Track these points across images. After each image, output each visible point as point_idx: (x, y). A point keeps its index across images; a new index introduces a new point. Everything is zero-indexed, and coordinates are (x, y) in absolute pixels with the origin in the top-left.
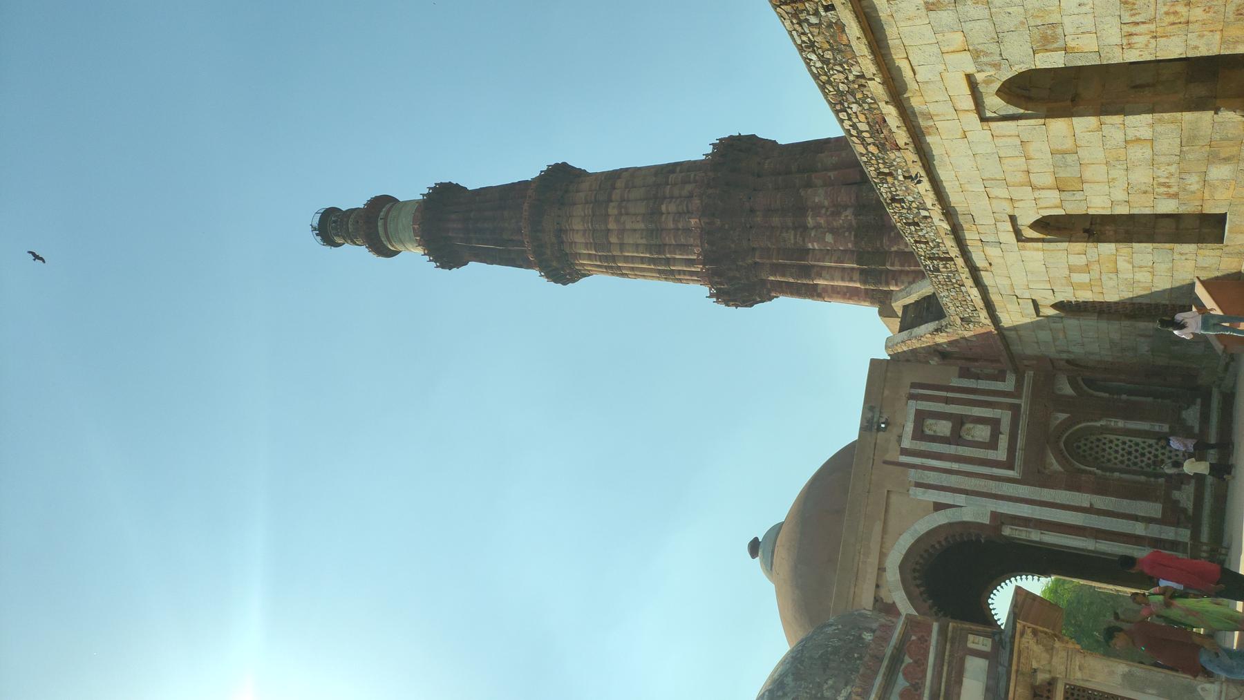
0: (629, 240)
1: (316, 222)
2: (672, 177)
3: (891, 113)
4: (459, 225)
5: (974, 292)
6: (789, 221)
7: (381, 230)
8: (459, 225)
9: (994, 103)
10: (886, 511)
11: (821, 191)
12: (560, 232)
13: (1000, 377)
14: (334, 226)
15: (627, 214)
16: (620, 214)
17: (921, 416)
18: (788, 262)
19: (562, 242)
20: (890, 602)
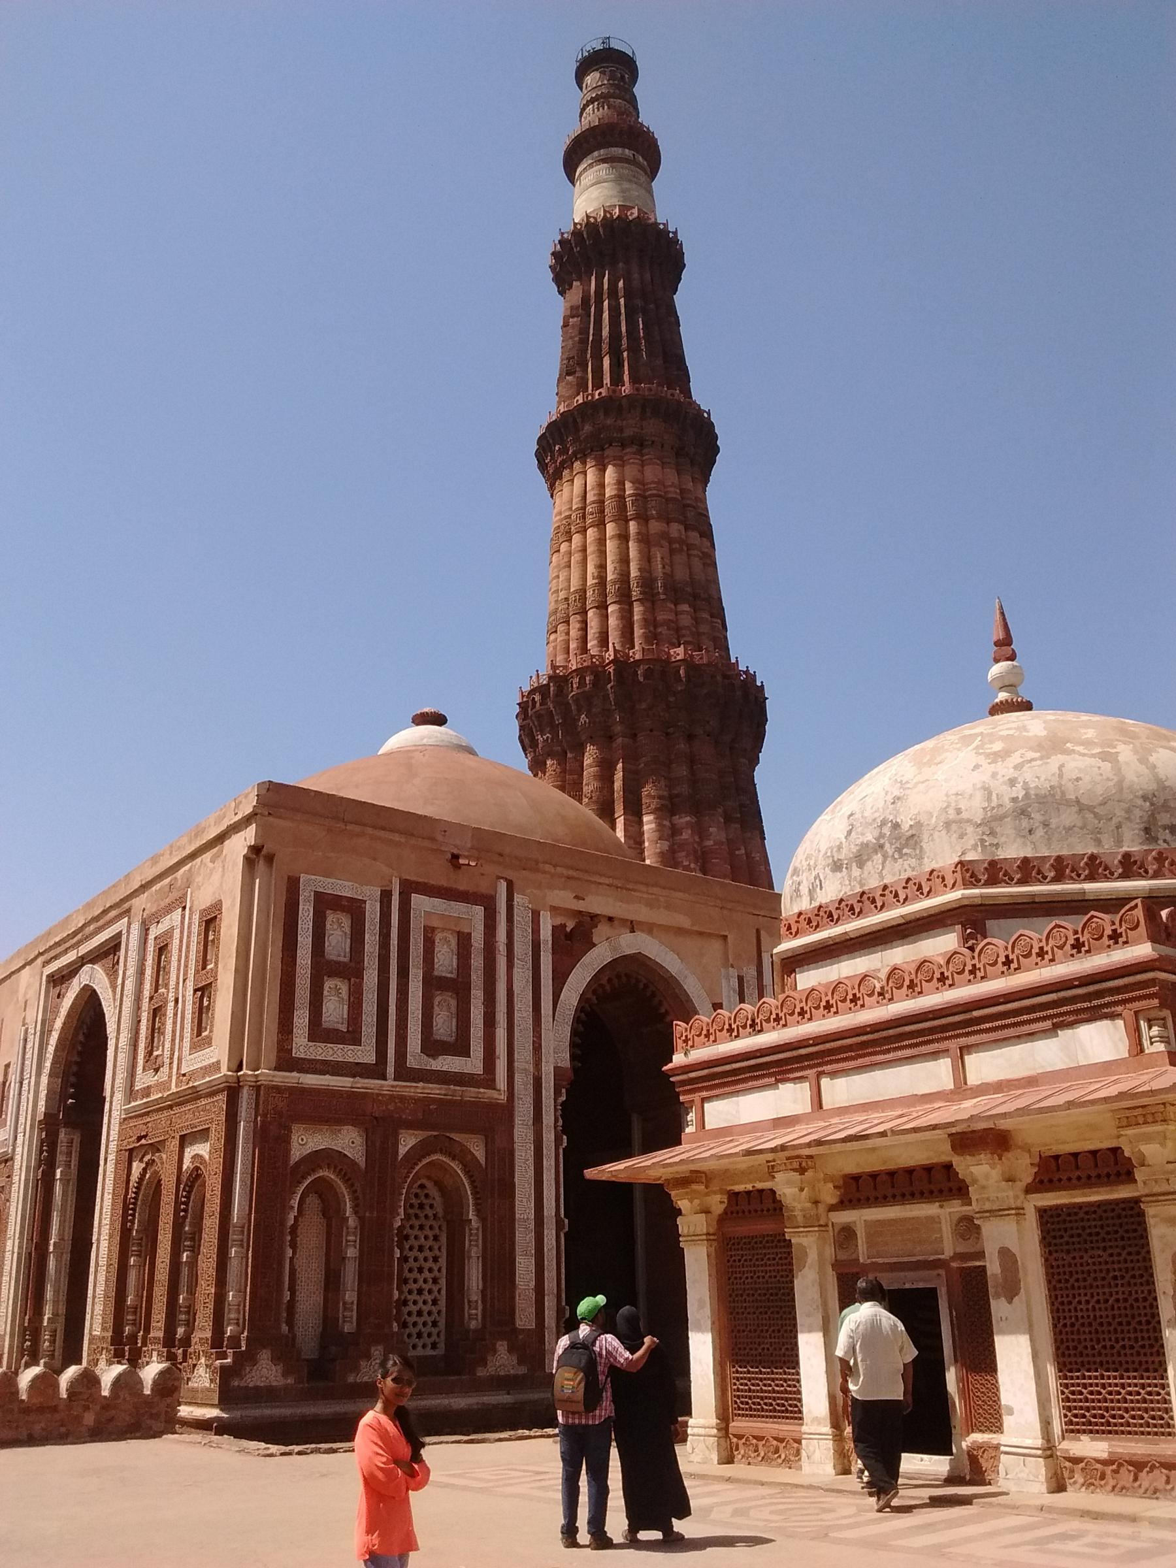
1: (615, 45)
6: (684, 789)
10: (701, 934)
11: (722, 837)
12: (640, 443)
14: (612, 68)
15: (672, 552)
16: (671, 541)
18: (618, 784)
19: (623, 446)
20: (595, 940)
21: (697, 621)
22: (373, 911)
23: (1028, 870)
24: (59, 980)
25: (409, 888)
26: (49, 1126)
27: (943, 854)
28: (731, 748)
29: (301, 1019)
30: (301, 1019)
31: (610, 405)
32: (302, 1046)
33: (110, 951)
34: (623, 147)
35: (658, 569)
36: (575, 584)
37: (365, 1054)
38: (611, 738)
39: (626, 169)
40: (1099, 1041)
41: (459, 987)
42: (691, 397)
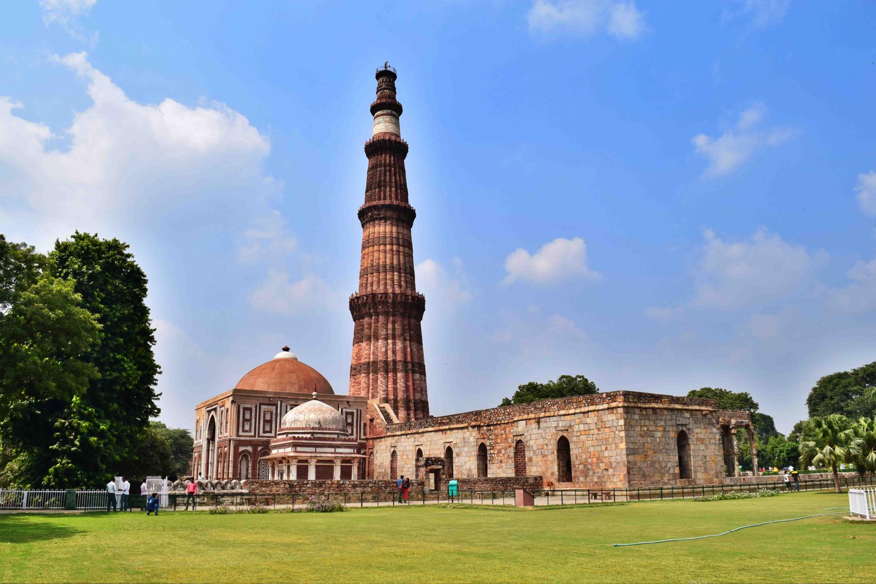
0: (382, 255)
2: (408, 276)
3: (447, 427)
4: (387, 154)
5: (399, 433)
6: (390, 332)
7: (385, 112)
8: (387, 154)
9: (448, 445)
12: (385, 219)
13: (365, 434)
14: (387, 77)
17: (352, 414)
21: (400, 277)
22: (254, 409)
23: (293, 429)
24: (209, 412)
25: (260, 405)
26: (208, 440)
27: (288, 426)
28: (409, 317)
29: (241, 429)
30: (241, 429)
31: (375, 207)
32: (241, 433)
33: (215, 409)
34: (387, 109)
35: (388, 262)
36: (365, 265)
37: (252, 434)
38: (371, 316)
39: (387, 118)
40: (289, 449)
41: (270, 422)
42: (407, 200)
